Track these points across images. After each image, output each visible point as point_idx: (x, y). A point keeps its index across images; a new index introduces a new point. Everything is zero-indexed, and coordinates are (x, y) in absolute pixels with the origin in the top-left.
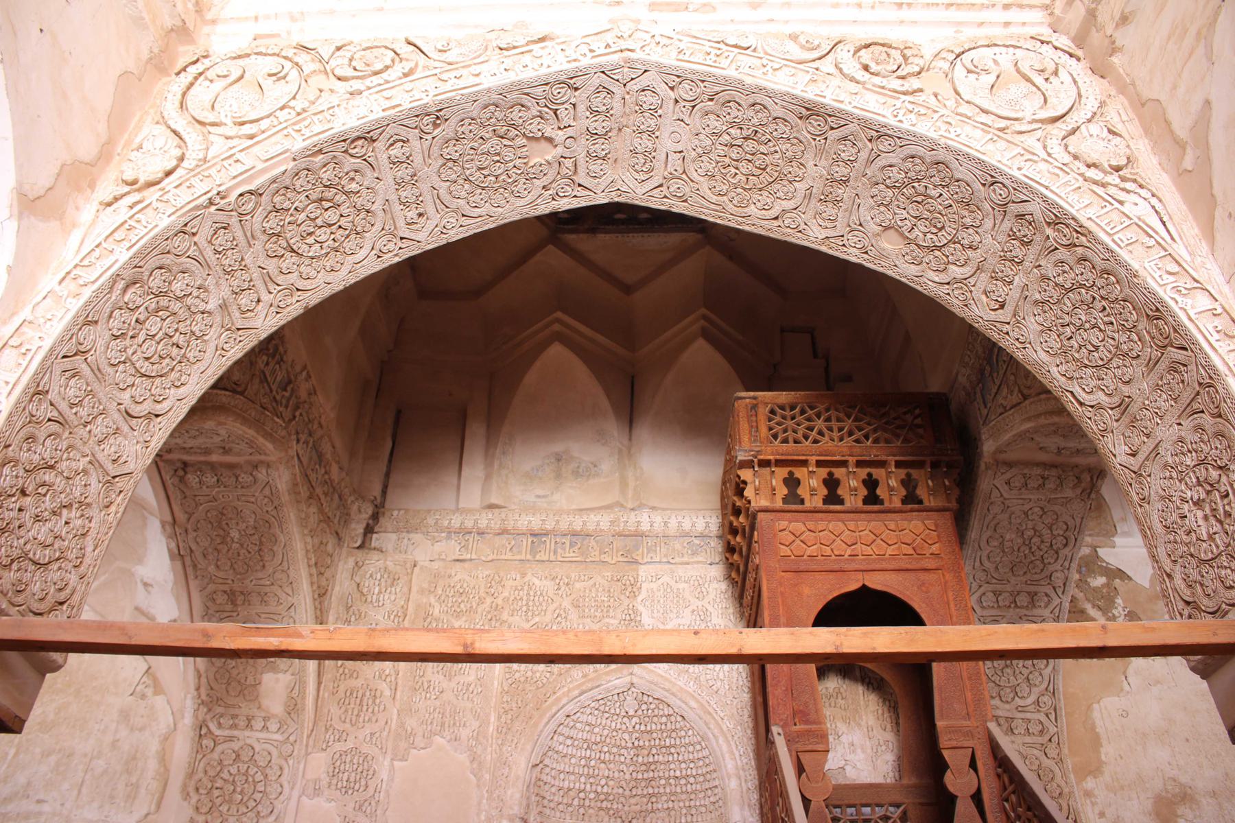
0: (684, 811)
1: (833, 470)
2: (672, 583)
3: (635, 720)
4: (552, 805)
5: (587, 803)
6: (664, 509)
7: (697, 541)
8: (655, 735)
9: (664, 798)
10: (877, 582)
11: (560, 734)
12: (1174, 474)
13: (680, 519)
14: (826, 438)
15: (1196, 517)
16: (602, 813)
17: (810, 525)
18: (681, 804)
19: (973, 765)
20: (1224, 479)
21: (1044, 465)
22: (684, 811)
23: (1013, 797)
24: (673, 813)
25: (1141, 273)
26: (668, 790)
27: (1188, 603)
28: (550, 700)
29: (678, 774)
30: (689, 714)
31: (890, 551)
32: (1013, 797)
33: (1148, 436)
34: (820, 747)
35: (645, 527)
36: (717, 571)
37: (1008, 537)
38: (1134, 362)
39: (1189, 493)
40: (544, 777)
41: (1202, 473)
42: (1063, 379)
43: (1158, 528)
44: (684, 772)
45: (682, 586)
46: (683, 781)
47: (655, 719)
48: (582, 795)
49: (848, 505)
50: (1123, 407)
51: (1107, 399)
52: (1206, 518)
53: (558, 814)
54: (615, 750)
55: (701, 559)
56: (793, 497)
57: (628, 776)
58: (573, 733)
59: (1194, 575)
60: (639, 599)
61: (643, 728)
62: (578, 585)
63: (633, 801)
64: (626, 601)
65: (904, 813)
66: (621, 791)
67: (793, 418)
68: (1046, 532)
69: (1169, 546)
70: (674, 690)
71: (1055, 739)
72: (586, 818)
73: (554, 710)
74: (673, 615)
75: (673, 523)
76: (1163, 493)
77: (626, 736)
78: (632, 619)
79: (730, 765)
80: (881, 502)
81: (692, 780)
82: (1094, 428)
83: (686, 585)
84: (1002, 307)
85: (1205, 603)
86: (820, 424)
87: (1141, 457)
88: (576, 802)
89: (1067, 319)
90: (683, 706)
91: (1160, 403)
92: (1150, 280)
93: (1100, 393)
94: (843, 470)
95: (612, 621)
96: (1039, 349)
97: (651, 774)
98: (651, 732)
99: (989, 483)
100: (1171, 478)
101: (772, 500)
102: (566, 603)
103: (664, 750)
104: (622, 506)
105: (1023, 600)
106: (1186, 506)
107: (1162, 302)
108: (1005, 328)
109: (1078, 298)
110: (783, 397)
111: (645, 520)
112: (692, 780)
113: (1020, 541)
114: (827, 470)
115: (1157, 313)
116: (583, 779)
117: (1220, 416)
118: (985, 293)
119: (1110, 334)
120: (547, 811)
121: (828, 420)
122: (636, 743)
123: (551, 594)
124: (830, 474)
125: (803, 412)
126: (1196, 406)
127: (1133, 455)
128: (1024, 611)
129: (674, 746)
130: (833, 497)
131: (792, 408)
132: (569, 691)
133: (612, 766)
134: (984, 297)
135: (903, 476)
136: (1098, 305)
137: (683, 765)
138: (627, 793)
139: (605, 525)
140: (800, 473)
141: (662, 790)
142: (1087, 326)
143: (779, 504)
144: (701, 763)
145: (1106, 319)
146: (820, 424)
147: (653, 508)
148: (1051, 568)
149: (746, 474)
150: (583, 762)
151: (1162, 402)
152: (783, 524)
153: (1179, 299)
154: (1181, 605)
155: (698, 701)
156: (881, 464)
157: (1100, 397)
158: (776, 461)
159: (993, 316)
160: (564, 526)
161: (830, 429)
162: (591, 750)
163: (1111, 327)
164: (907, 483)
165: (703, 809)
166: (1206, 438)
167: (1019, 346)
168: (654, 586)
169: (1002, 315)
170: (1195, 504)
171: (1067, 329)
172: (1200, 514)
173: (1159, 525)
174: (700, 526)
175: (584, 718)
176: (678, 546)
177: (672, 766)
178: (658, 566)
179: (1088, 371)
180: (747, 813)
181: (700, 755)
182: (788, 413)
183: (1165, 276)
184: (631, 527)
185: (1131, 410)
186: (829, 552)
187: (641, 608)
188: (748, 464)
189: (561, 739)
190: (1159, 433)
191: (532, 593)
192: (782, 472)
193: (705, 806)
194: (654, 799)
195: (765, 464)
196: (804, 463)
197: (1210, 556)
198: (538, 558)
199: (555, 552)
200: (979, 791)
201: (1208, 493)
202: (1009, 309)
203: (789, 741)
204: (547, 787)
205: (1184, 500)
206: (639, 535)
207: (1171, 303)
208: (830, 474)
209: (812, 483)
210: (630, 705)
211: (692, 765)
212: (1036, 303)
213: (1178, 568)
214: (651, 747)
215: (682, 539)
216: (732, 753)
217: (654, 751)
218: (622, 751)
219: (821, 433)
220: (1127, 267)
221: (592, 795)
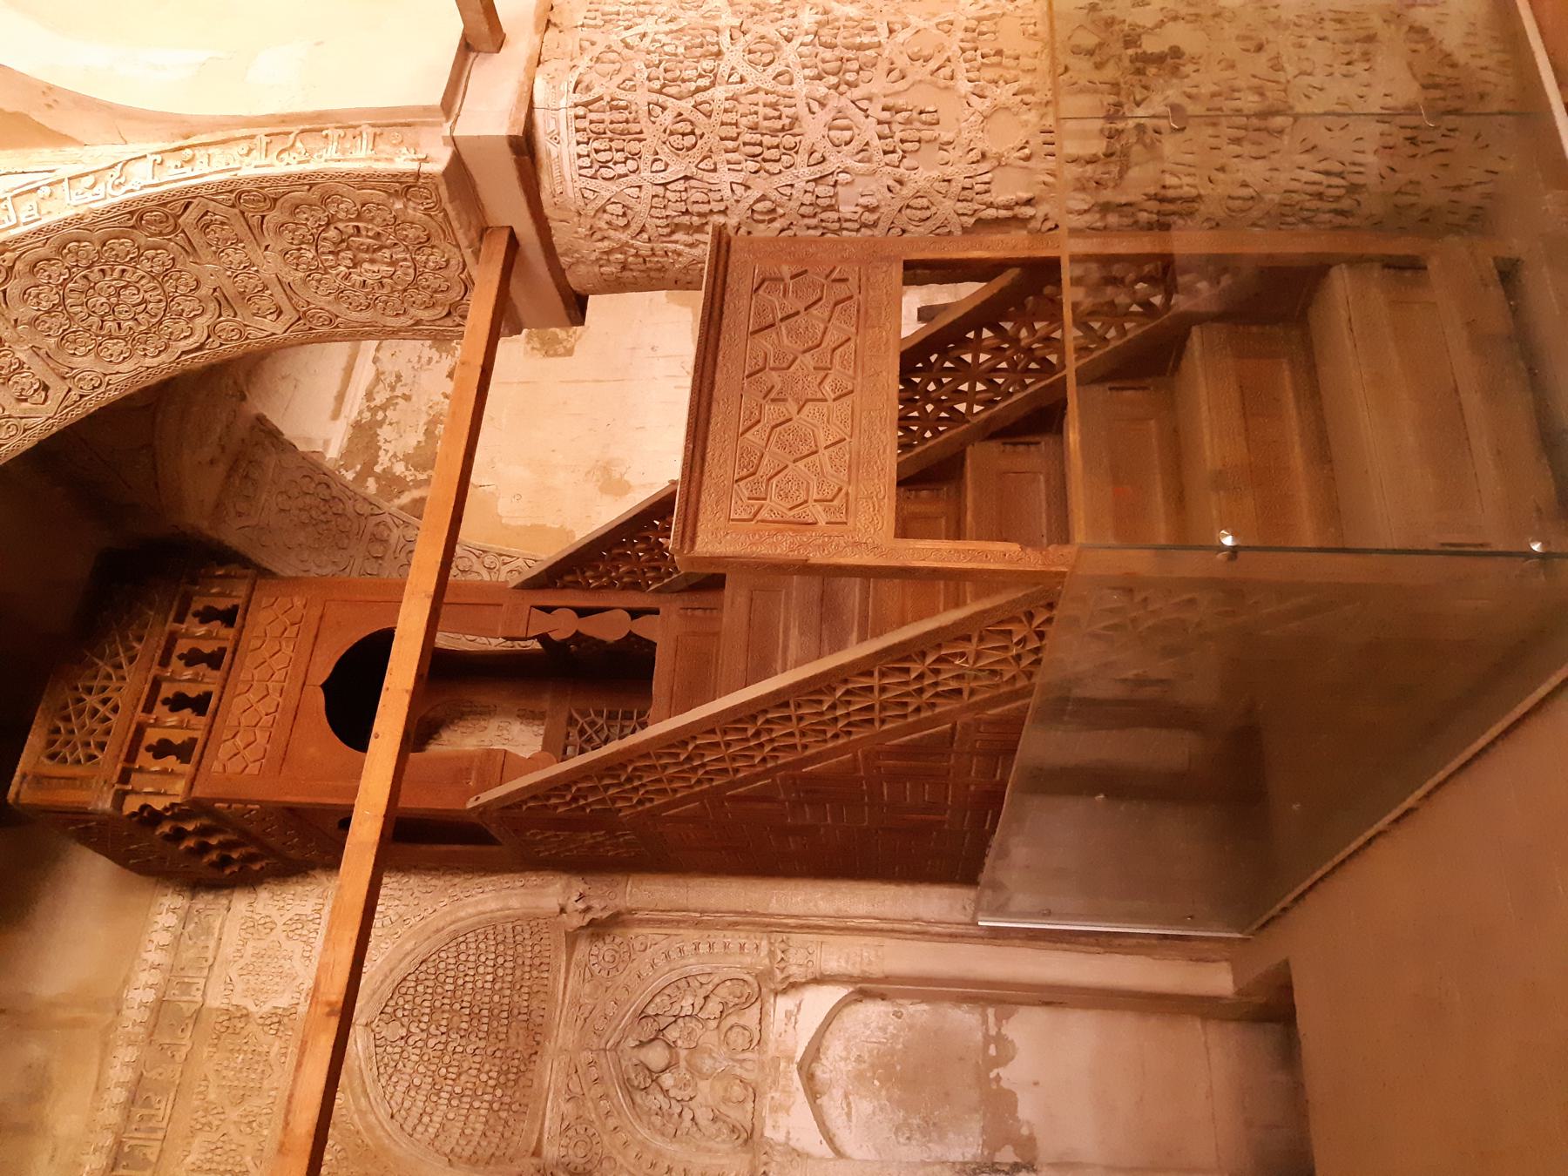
0: (535, 973)
1: (161, 697)
2: (242, 963)
3: (413, 1029)
4: (503, 1145)
5: (507, 1100)
6: (131, 969)
7: (191, 927)
8: (438, 1004)
9: (516, 998)
10: (323, 669)
11: (414, 1129)
12: (318, 276)
13: (152, 947)
14: (115, 696)
15: (370, 272)
16: (521, 1082)
17: (227, 735)
18: (527, 976)
19: (548, 610)
20: (341, 226)
21: (232, 470)
22: (535, 973)
23: (588, 574)
24: (535, 989)
25: (81, 211)
26: (508, 992)
27: (449, 314)
28: (367, 1140)
29: (489, 978)
30: (424, 949)
31: (288, 650)
32: (588, 574)
33: (266, 287)
34: (500, 758)
35: (150, 996)
36: (241, 903)
37: (302, 539)
38: (179, 267)
39: (342, 268)
40: (467, 1153)
41: (326, 246)
42: (163, 356)
43: (366, 316)
44: (490, 970)
45: (249, 950)
46: (500, 972)
47: (418, 1000)
48: (496, 1106)
49: (215, 689)
50: (223, 302)
51: (207, 316)
52: (372, 261)
53: (516, 1138)
54: (446, 1059)
55: (217, 925)
56: (183, 752)
57: (482, 1044)
58: (415, 1112)
59: (424, 296)
60: (252, 1008)
61: (426, 1019)
62: (212, 1097)
63: (513, 1039)
64: (252, 1027)
65: (578, 711)
66: (498, 1054)
67: (72, 732)
68: (308, 500)
69: (388, 312)
70: (386, 968)
71: (530, 563)
72: (524, 1101)
73: (379, 1132)
74: (287, 964)
75: (155, 957)
76: (331, 297)
77: (432, 1042)
78: (278, 1020)
79: (493, 905)
80: (223, 650)
81: (500, 960)
82: (233, 344)
83: (251, 944)
84: (46, 388)
85: (455, 295)
86: (91, 701)
87: (286, 306)
88: (504, 1114)
89: (95, 319)
90: (409, 958)
91: (237, 258)
92: (94, 206)
93: (198, 320)
94: (164, 686)
95: (275, 1049)
96: (117, 368)
97: (485, 1012)
98: (432, 1008)
99: (232, 535)
100: (319, 281)
101: (181, 775)
102: (234, 1114)
103: (459, 993)
104: (109, 1026)
105: (378, 550)
106: (354, 277)
107: (125, 204)
108: (74, 395)
109: (75, 295)
110: (35, 741)
111: (140, 995)
112: (500, 960)
113: (310, 529)
114: (159, 703)
115: (136, 216)
116: (477, 1104)
117: (275, 200)
118: (19, 400)
119: (134, 278)
120: (511, 1151)
121: (89, 691)
122: (443, 1029)
123: (215, 1136)
124: (166, 702)
125: (67, 719)
126: (255, 221)
127: (281, 313)
128: (390, 552)
129: (456, 978)
130: (200, 704)
131: (58, 731)
132: (359, 1111)
133: (466, 1065)
134: (24, 405)
135: (197, 620)
136: (95, 275)
137: (481, 970)
138: (502, 1045)
139: (127, 1054)
140: (152, 736)
141: (506, 1000)
142: (114, 300)
143: (188, 768)
144: (482, 946)
145: (116, 275)
146: (91, 701)
147: (126, 982)
148: (350, 510)
149: (132, 805)
150: (455, 1103)
151: (235, 257)
152: (217, 766)
153: (128, 187)
154: (449, 322)
155: (408, 939)
156: (172, 639)
157: (202, 323)
158: (126, 760)
159: (52, 405)
160: (114, 1116)
161: (104, 689)
162: (440, 1090)
163: (127, 275)
164: (207, 616)
165: (537, 948)
166: (292, 226)
167: (102, 389)
168: (239, 987)
169: (57, 393)
170: (355, 266)
171: (108, 324)
172: (366, 265)
173: (364, 314)
174: (171, 920)
175: (398, 1097)
176: (191, 954)
177: (479, 984)
178: (212, 980)
179: (167, 322)
180: (551, 890)
181: (473, 946)
182: (61, 738)
183: (95, 190)
184: (145, 1015)
185: (230, 291)
186: (270, 718)
187: (267, 1008)
188: (120, 797)
189: (420, 1129)
190: (267, 273)
191: (207, 1166)
192: (144, 758)
193: (533, 946)
194: (516, 1011)
195: (125, 777)
196: (140, 730)
197: (411, 271)
198: (153, 1158)
199: (154, 1130)
200: (576, 609)
201: (348, 248)
202: (51, 380)
203: (486, 788)
204: (479, 1152)
205: (347, 277)
206: (160, 1007)
207: (130, 195)
208: (166, 702)
209: (172, 726)
210: (395, 1031)
211: (483, 959)
212: (58, 345)
213: (412, 311)
214: (452, 1010)
215: (182, 947)
216: (477, 903)
217: (457, 1006)
218: (450, 1048)
219: (105, 702)
220: (67, 223)
221: (499, 1092)
